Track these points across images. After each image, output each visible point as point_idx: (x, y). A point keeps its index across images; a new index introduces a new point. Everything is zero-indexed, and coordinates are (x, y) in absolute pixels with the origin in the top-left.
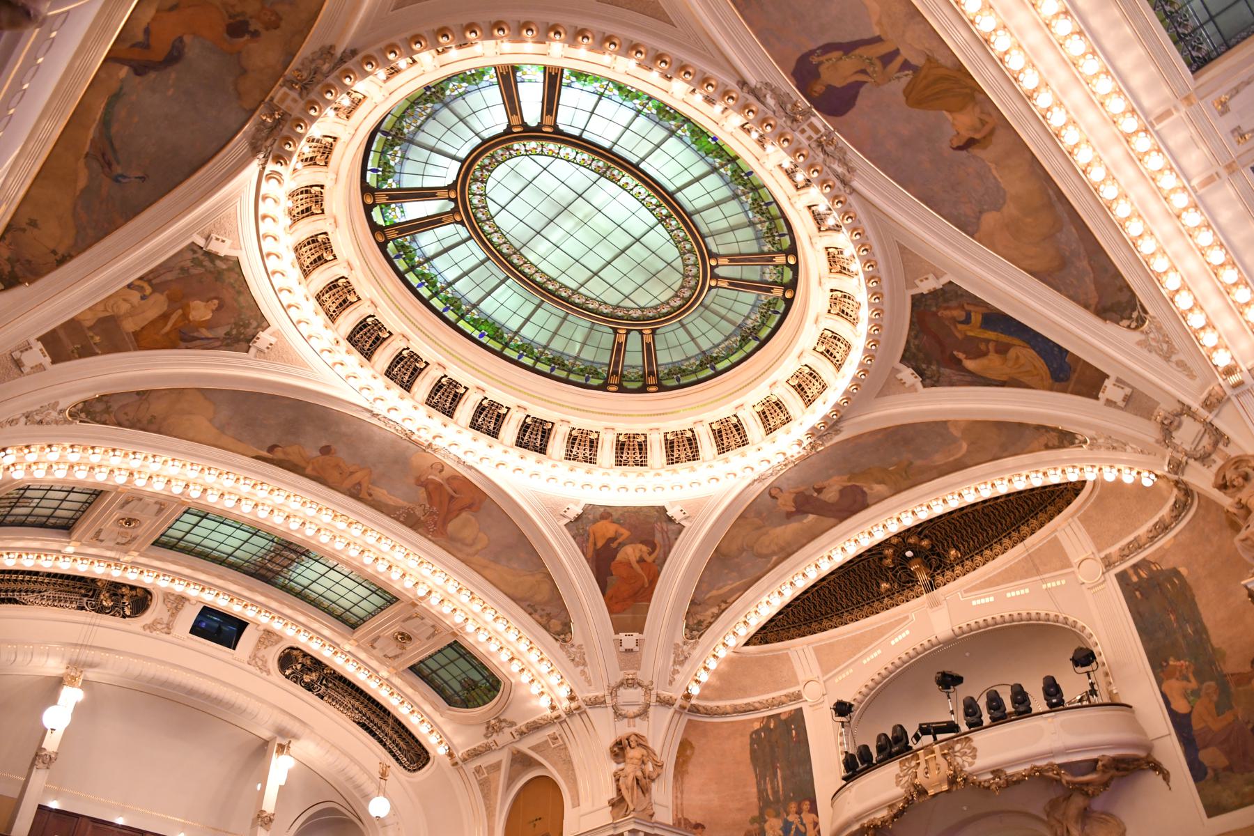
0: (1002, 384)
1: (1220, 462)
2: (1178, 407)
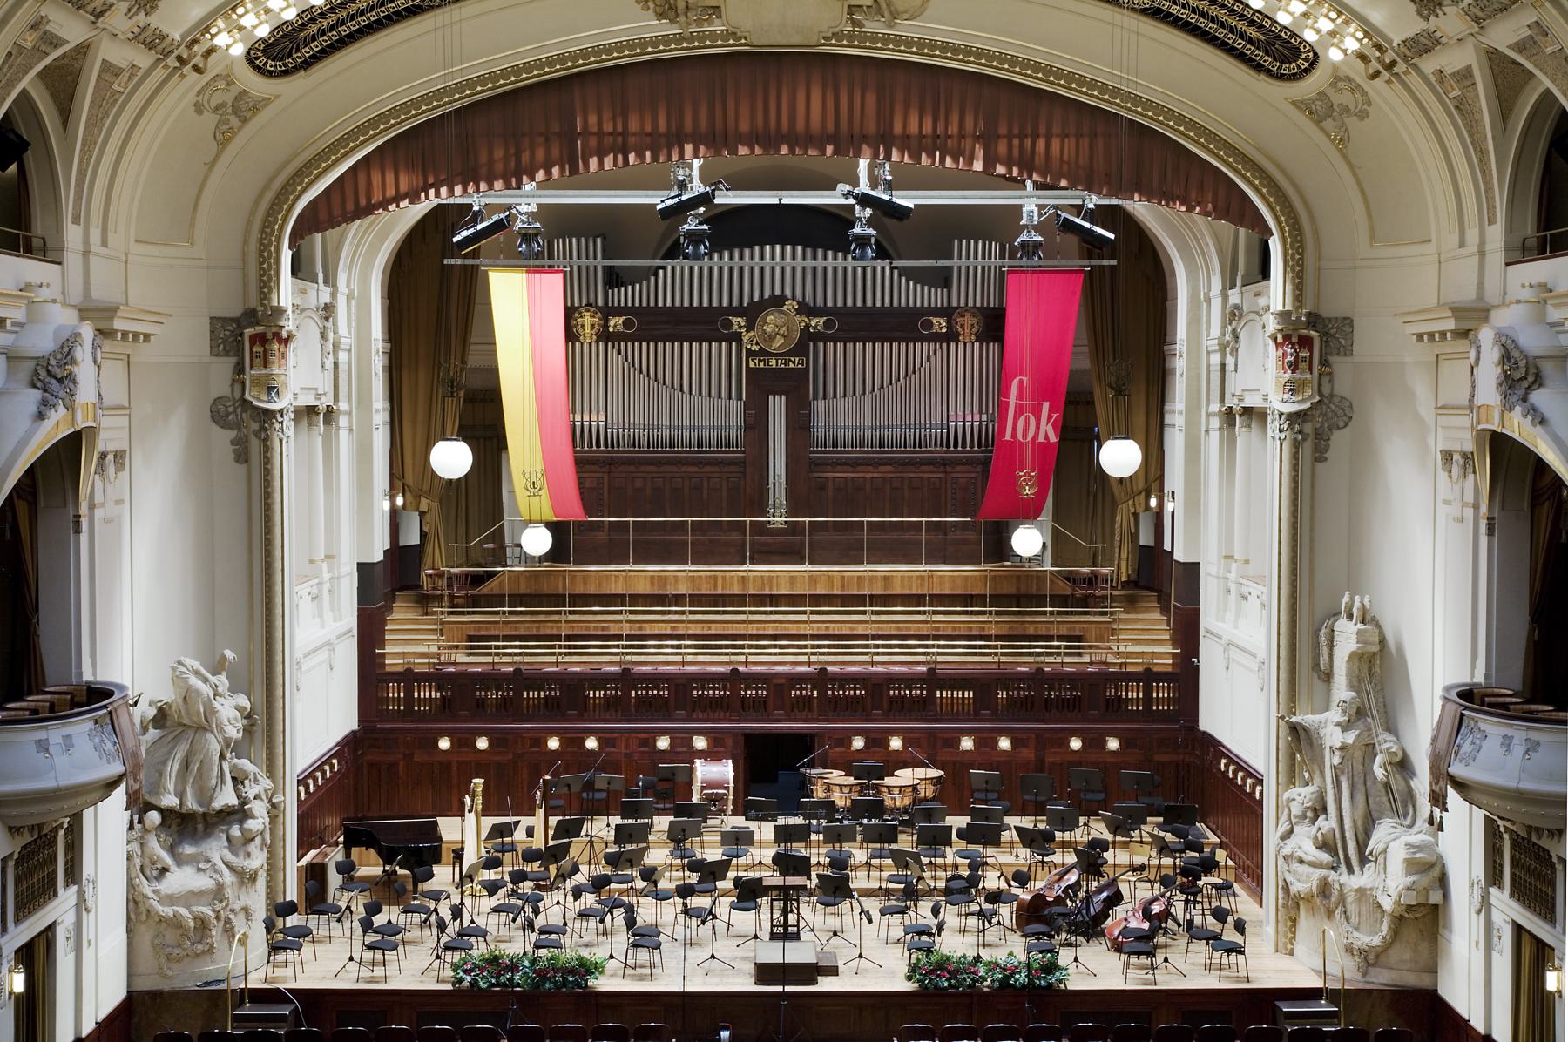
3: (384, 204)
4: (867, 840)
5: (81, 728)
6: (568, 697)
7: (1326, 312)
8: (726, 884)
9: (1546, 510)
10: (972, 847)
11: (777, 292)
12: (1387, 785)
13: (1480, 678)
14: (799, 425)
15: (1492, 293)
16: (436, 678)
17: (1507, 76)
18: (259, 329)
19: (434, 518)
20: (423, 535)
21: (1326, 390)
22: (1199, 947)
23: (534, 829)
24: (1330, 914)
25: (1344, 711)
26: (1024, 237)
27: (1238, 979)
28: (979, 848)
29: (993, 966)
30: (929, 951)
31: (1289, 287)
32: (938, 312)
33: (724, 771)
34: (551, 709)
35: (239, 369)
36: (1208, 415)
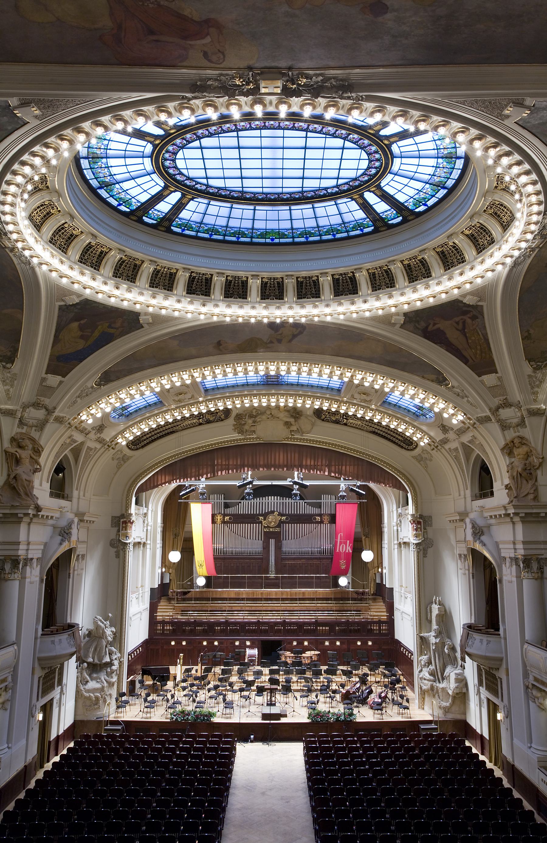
0: (56, 336)
1: (24, 431)
2: (50, 407)
3: (161, 485)
4: (297, 674)
5: (64, 637)
6: (210, 629)
7: (425, 514)
8: (254, 688)
9: (488, 571)
10: (328, 676)
12: (449, 655)
13: (473, 622)
14: (278, 547)
15: (469, 509)
16: (172, 623)
17: (467, 450)
18: (125, 519)
19: (173, 575)
20: (170, 580)
21: (426, 537)
22: (396, 707)
23: (197, 670)
24: (434, 696)
25: (435, 632)
26: (341, 494)
27: (408, 718)
28: (330, 676)
29: (334, 714)
30: (314, 709)
31: (414, 507)
32: (318, 515)
33: (255, 652)
34: (205, 633)
35: (119, 531)
36: (394, 544)
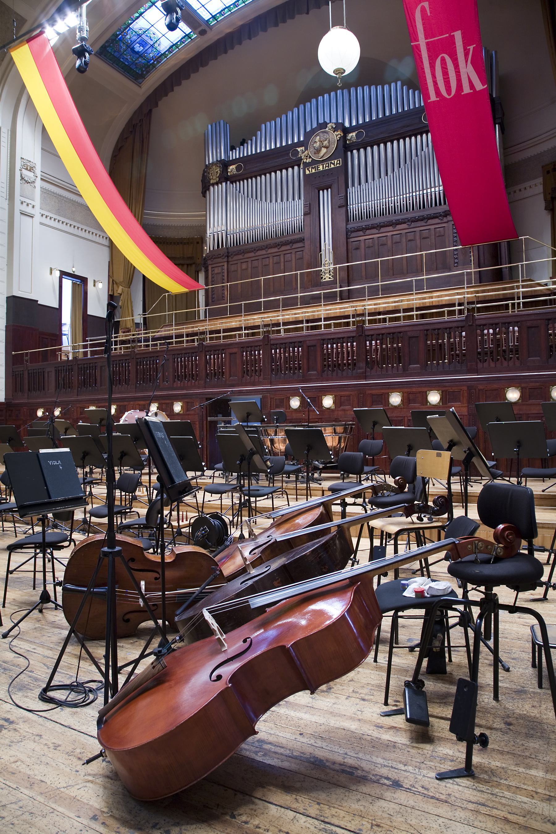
11: (321, 121)
